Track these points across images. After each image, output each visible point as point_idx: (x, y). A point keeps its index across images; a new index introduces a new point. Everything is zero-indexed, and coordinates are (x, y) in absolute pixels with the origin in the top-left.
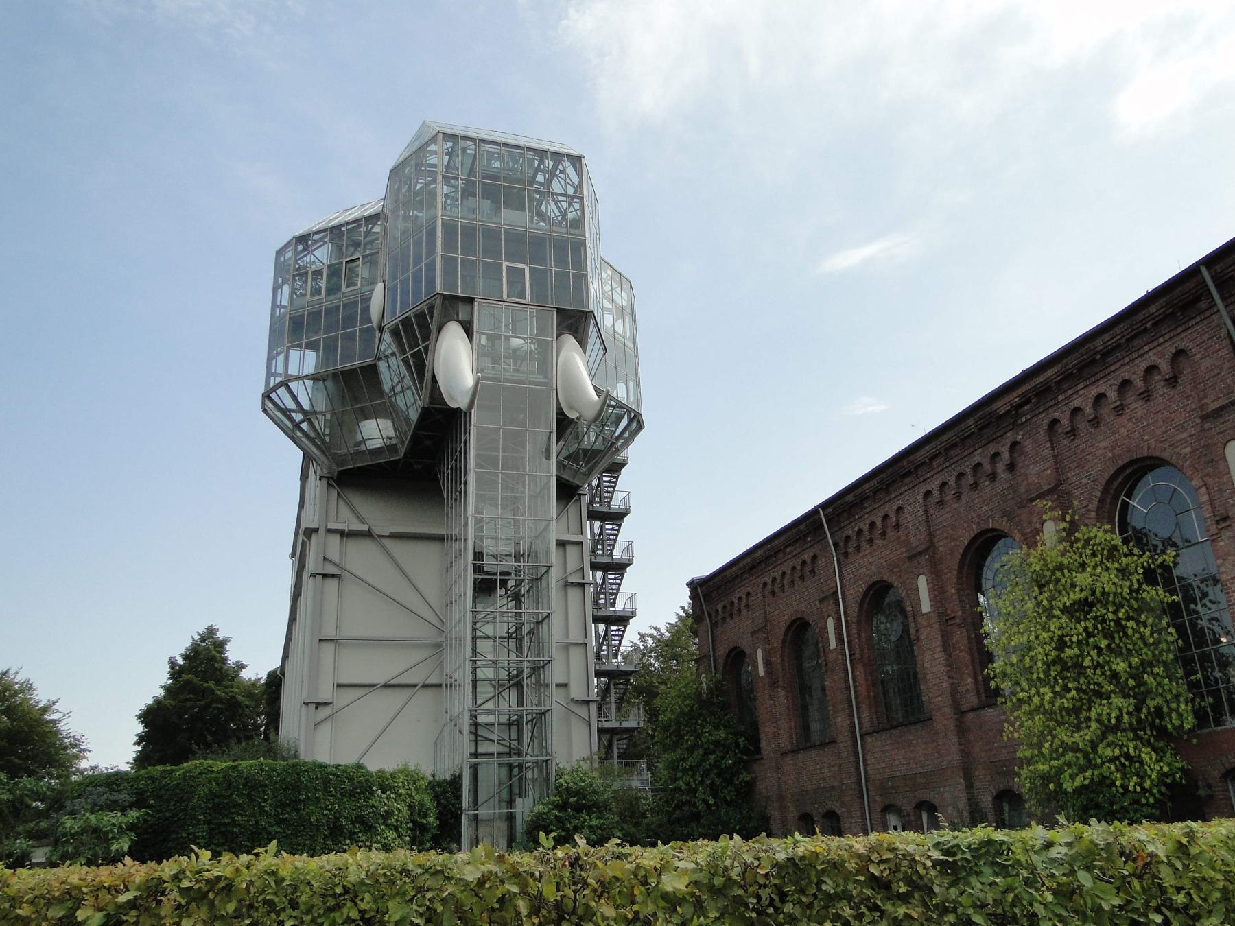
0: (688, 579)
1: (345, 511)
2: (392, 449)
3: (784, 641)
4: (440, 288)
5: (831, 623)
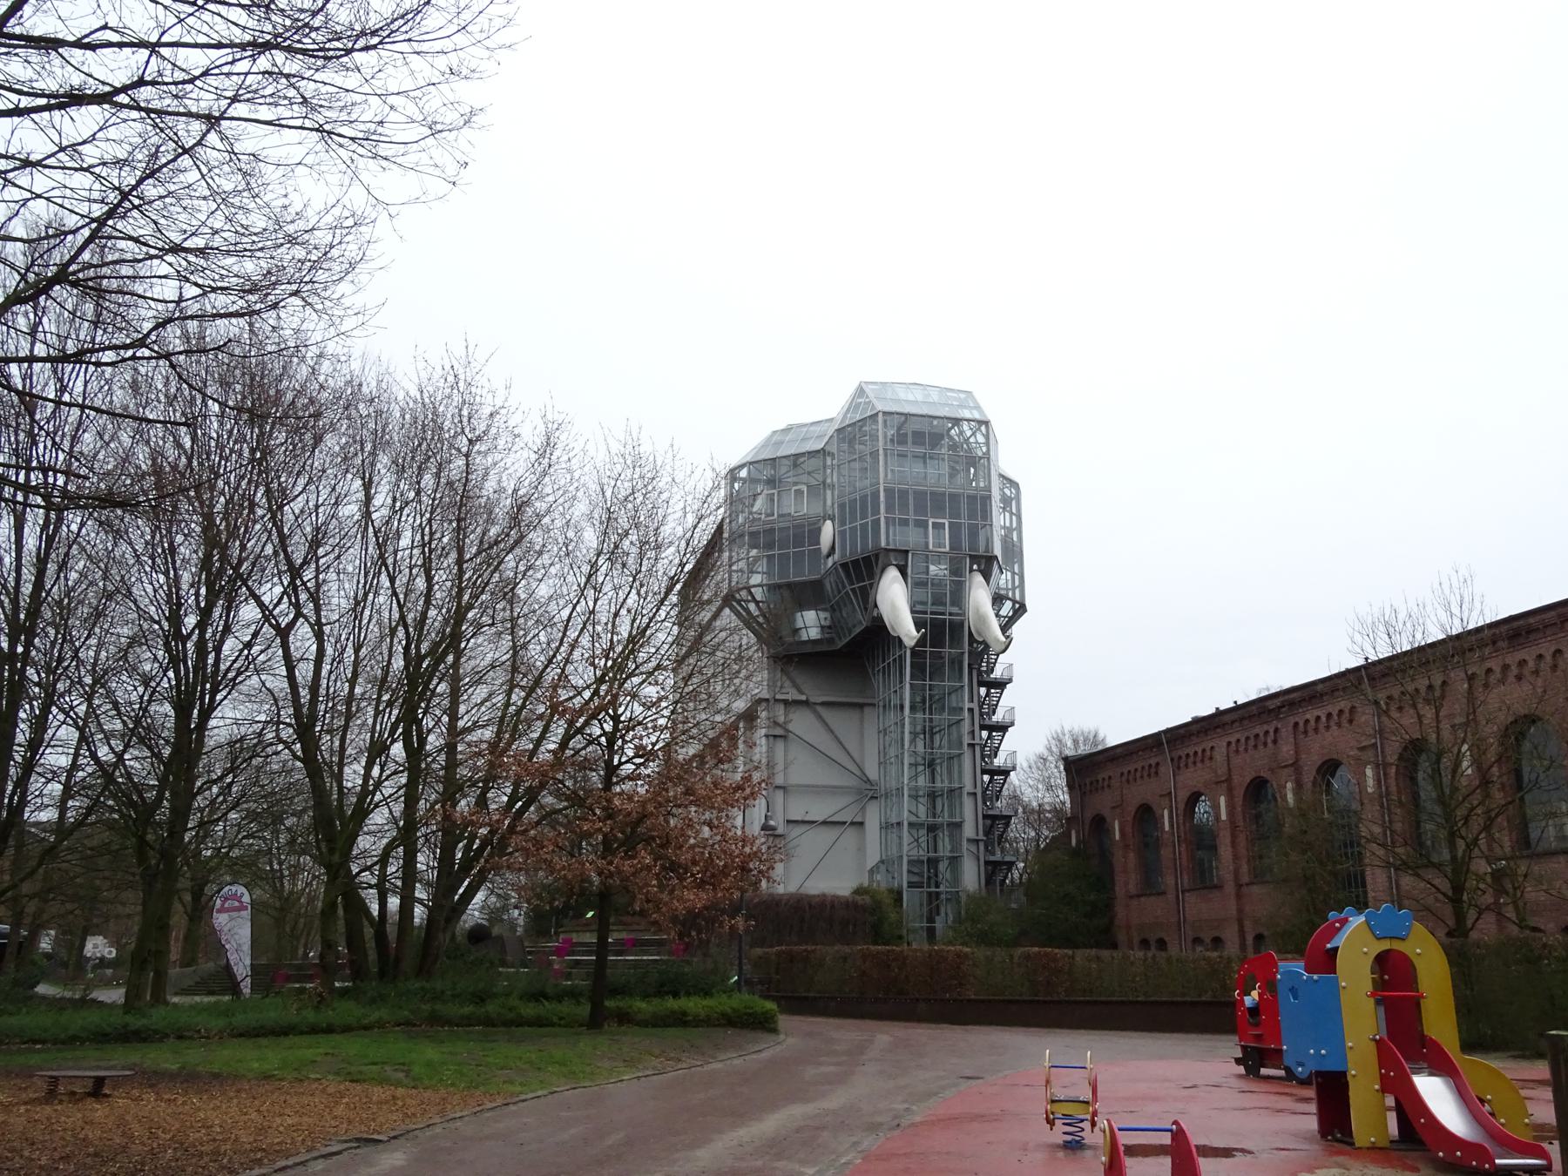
2: (831, 641)
4: (883, 544)
5: (1166, 813)
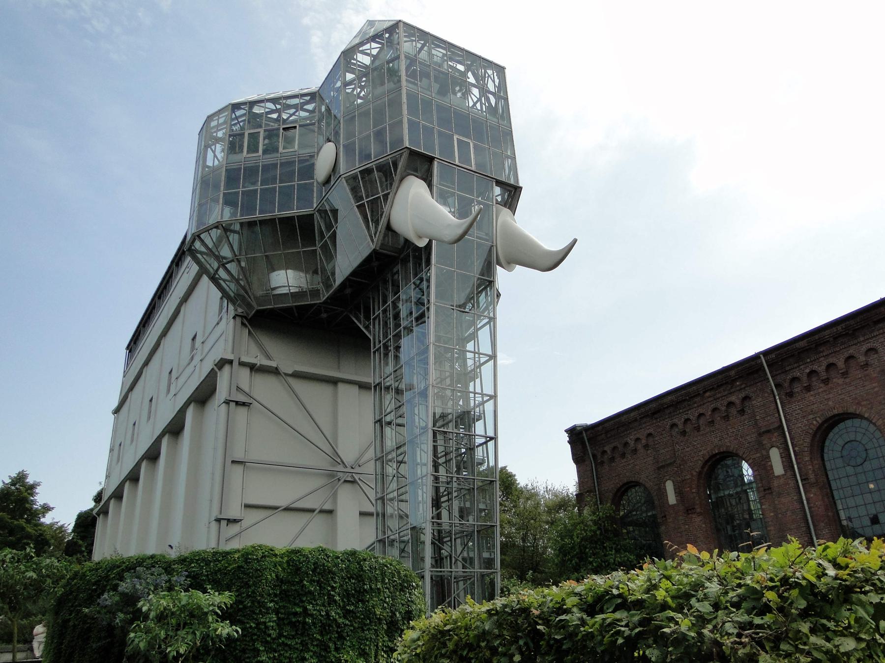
0: (569, 425)
1: (254, 349)
3: (700, 473)
